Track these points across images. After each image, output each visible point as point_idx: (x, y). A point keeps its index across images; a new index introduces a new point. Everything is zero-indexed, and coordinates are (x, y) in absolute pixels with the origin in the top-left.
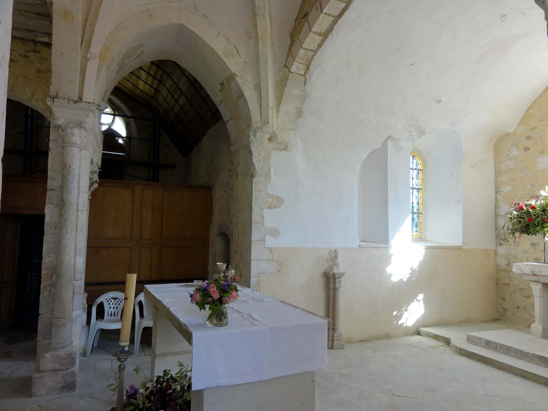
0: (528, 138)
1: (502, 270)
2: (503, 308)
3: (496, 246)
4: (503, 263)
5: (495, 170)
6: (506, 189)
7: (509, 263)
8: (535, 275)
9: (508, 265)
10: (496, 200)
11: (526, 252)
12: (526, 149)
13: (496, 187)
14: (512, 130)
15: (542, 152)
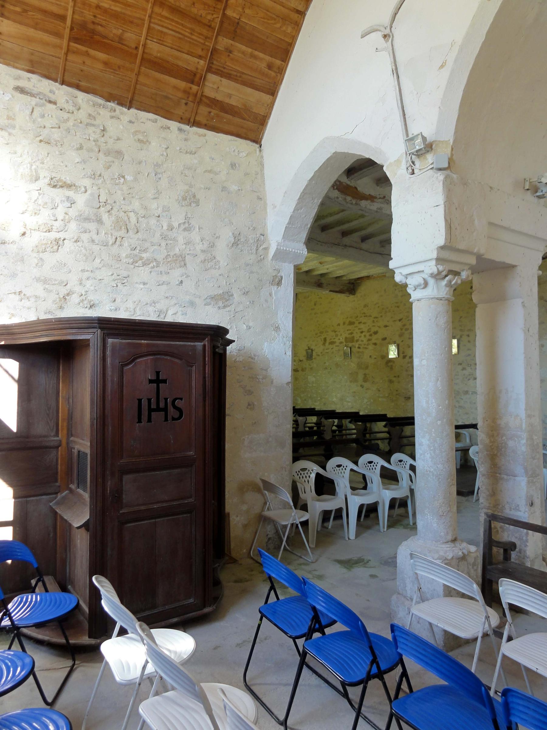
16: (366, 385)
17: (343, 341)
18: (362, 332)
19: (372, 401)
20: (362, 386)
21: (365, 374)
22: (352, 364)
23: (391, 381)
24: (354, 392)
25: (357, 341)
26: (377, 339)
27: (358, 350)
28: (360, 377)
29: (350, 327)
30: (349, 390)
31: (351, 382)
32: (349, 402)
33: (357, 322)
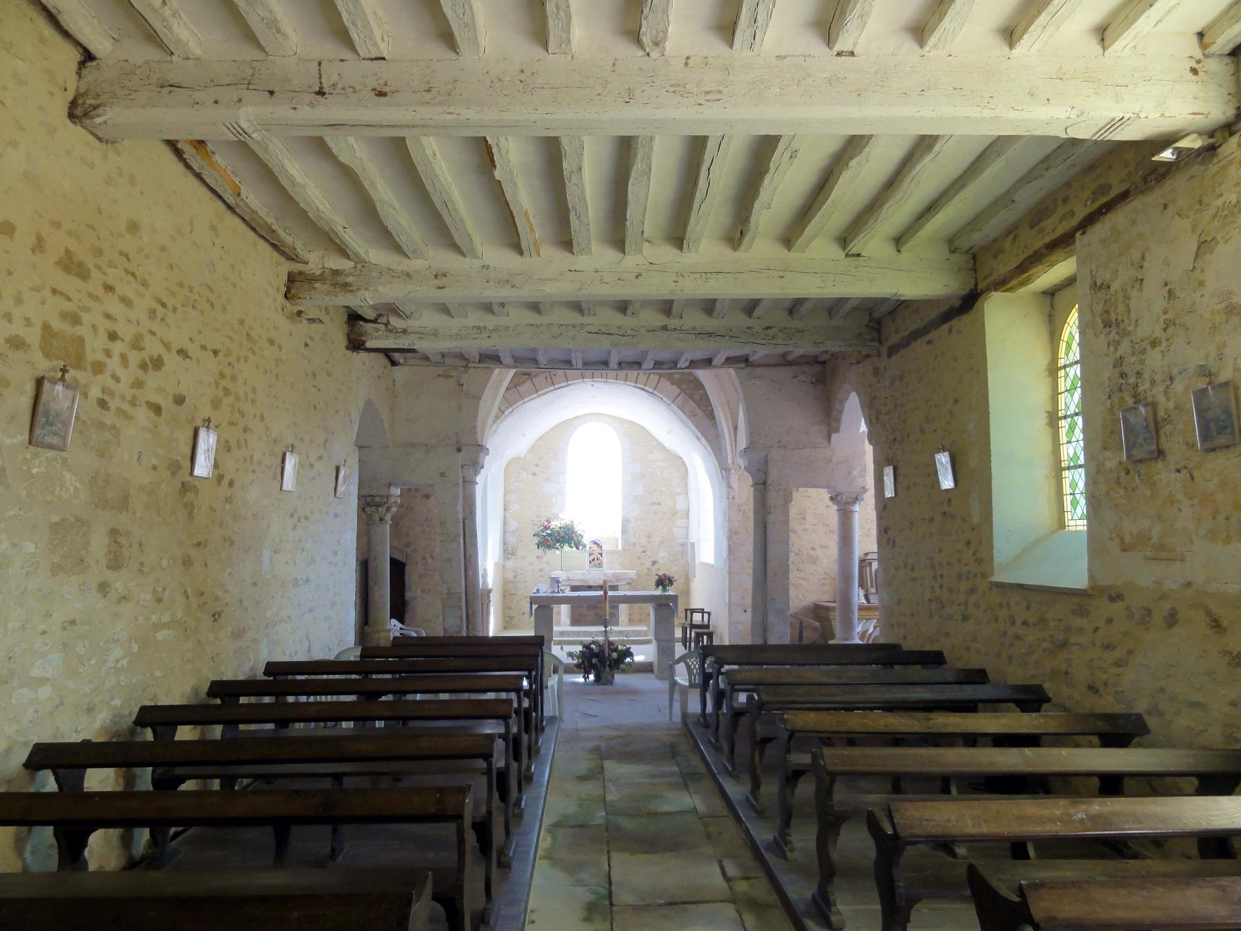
0: (536, 465)
1: (509, 582)
2: (509, 617)
3: (504, 560)
4: (510, 576)
5: (505, 489)
6: (515, 508)
7: (516, 575)
8: (569, 580)
9: (515, 576)
10: (505, 518)
11: (532, 564)
12: (534, 474)
13: (505, 505)
14: (523, 456)
15: (547, 479)
16: (119, 582)
17: (33, 336)
18: (113, 336)
19: (135, 647)
20: (103, 587)
21: (114, 533)
22: (68, 476)
23: (187, 562)
24: (73, 623)
25: (98, 368)
26: (159, 390)
27: (98, 413)
28: (99, 544)
29: (69, 283)
30: (49, 615)
31: (56, 569)
32: (42, 681)
33: (96, 279)
